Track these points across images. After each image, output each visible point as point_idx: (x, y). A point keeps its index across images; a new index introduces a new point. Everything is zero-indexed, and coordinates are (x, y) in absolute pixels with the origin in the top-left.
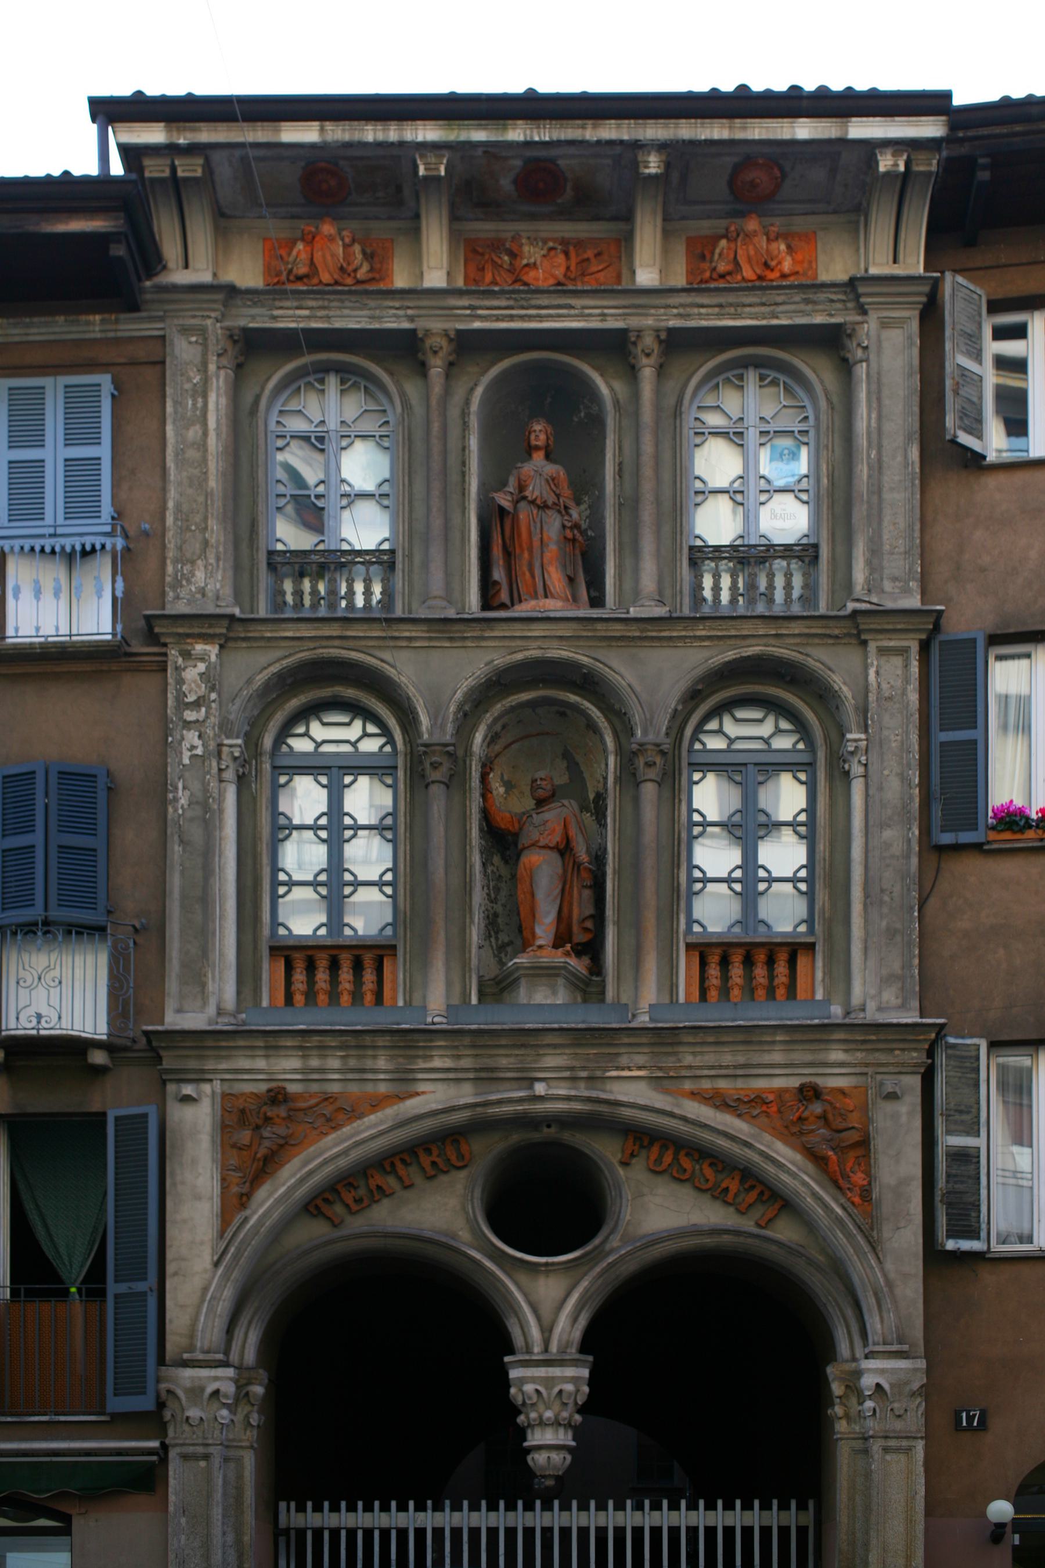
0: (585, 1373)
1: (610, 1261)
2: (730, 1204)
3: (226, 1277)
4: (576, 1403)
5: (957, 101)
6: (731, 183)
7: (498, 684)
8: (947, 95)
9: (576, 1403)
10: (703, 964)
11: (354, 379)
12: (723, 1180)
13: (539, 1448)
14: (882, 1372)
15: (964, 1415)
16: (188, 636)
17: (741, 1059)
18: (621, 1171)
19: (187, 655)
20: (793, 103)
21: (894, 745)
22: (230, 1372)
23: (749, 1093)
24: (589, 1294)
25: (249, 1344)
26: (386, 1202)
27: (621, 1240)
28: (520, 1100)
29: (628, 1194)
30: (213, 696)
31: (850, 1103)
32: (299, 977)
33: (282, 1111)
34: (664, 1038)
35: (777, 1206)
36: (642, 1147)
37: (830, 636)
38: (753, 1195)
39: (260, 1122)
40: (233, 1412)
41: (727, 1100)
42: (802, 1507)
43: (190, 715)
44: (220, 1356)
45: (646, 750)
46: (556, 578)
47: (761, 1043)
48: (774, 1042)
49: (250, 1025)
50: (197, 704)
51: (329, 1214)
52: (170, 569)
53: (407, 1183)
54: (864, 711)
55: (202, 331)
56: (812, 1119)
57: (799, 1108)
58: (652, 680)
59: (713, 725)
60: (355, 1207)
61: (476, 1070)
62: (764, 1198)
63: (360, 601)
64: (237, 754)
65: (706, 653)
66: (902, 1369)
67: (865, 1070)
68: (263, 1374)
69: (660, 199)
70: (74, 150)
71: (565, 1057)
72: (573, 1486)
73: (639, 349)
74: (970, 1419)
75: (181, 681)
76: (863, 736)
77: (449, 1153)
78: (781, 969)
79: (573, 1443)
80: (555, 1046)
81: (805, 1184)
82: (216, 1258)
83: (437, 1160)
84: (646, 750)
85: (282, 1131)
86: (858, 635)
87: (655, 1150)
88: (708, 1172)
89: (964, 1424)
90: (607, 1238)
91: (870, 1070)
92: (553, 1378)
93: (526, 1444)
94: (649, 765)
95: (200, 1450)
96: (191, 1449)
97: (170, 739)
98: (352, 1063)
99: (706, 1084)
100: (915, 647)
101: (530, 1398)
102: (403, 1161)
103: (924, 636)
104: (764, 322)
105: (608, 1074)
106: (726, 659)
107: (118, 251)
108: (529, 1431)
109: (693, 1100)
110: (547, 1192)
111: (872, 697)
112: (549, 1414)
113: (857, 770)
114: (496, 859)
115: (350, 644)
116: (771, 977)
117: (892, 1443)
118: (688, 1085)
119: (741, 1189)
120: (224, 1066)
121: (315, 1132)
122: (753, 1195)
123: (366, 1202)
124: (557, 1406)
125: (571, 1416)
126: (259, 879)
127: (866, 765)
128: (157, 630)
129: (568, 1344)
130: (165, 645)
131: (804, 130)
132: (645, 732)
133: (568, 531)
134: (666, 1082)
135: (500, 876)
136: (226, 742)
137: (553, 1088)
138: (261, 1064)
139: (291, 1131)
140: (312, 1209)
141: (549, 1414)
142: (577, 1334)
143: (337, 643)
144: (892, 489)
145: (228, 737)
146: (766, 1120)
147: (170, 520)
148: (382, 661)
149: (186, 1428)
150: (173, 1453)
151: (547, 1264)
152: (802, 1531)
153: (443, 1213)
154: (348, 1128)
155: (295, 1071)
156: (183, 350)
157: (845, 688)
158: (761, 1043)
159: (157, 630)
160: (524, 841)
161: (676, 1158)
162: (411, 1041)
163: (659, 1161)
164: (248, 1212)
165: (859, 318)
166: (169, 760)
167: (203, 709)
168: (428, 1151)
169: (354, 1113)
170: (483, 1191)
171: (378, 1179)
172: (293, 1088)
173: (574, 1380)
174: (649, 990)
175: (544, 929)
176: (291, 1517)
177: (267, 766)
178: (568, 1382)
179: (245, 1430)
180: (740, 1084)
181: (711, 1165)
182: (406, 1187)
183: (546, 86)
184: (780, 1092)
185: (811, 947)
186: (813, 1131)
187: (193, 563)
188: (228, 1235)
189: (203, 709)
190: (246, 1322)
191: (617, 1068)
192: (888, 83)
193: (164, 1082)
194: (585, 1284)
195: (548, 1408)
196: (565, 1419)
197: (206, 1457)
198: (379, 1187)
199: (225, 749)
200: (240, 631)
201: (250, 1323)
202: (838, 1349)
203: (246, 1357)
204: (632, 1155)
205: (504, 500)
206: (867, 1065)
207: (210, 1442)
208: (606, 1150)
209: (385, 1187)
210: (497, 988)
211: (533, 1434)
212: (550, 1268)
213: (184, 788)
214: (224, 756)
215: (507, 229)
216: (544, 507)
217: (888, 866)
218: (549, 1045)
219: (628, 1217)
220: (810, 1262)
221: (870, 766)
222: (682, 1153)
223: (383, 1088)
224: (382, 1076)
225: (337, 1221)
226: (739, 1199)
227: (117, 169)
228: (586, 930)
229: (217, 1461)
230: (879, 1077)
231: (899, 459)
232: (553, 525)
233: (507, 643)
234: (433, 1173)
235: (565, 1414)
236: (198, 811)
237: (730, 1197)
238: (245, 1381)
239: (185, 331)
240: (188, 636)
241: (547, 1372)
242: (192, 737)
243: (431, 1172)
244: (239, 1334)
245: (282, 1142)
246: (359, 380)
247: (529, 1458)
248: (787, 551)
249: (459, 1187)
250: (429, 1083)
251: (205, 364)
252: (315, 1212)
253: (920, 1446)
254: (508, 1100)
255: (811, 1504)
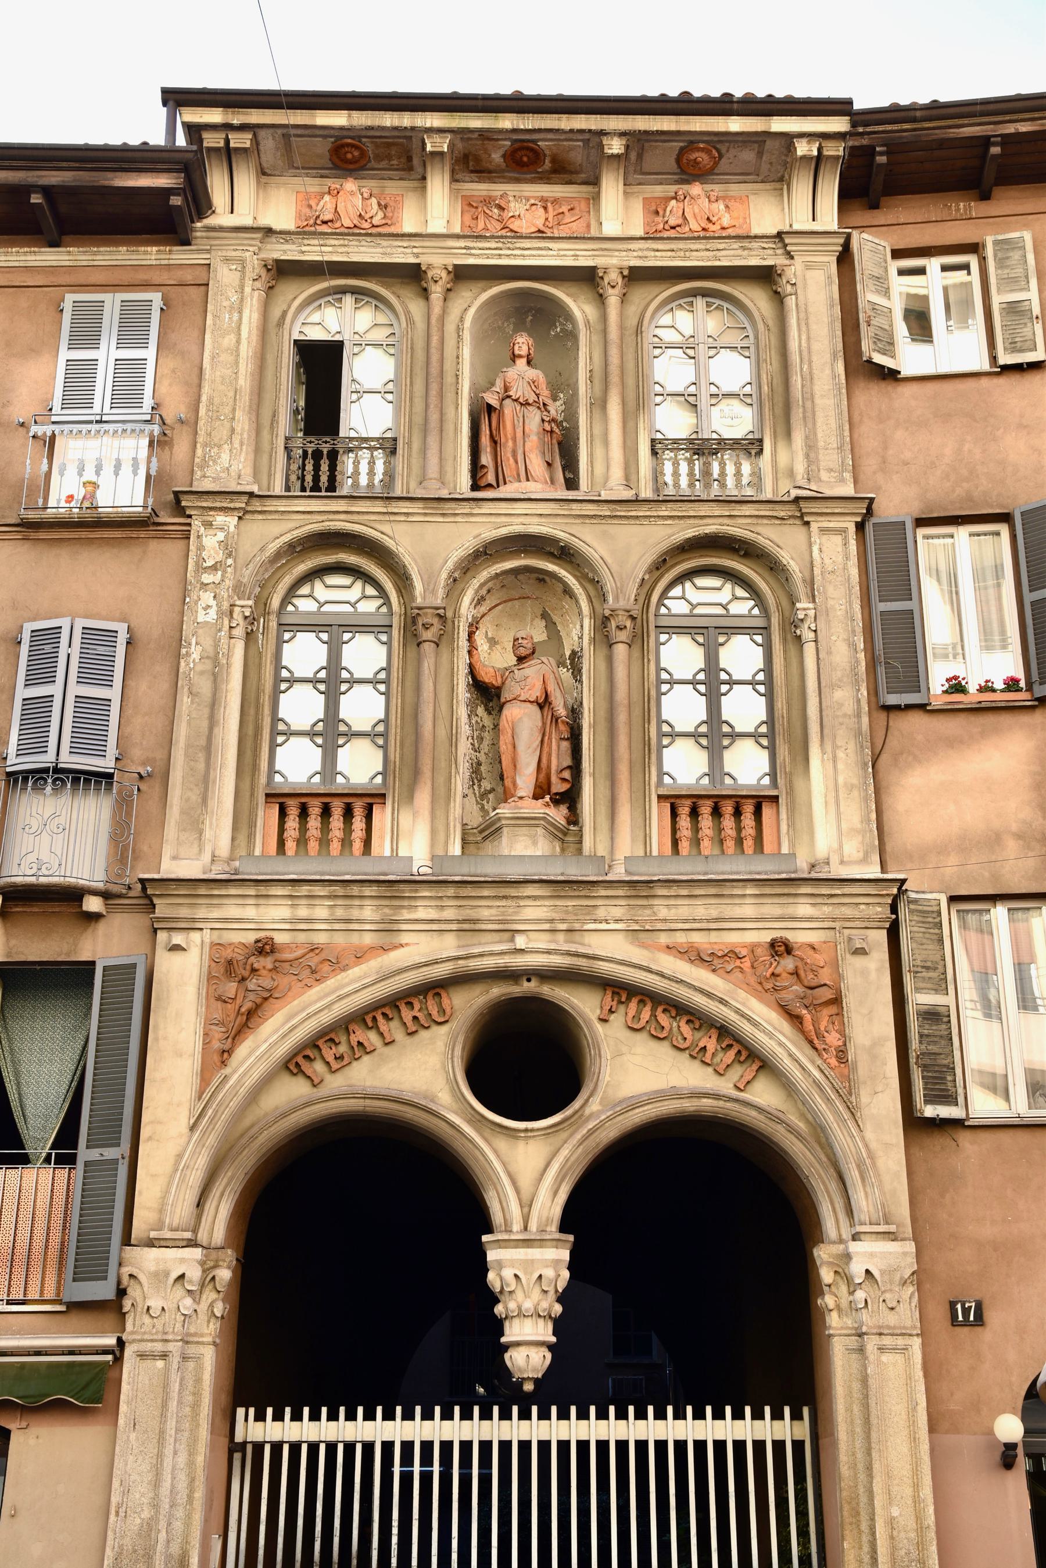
0: (565, 1255)
1: (590, 1127)
2: (708, 1065)
3: (200, 1142)
4: (557, 1291)
5: (857, 106)
6: (678, 161)
7: (485, 553)
8: (849, 102)
9: (557, 1291)
10: (674, 814)
11: (367, 299)
12: (700, 1039)
13: (518, 1344)
14: (872, 1255)
15: (959, 1306)
16: (211, 509)
17: (714, 913)
18: (599, 1027)
19: (208, 525)
20: (725, 106)
21: (839, 613)
22: (197, 1253)
23: (723, 947)
24: (569, 1163)
25: (219, 1219)
26: (366, 1058)
27: (601, 1103)
28: (502, 953)
29: (607, 1052)
30: (230, 561)
31: (820, 959)
32: (292, 823)
33: (267, 962)
34: (639, 888)
35: (755, 1067)
36: (620, 1002)
37: (777, 518)
38: (731, 1054)
39: (246, 974)
40: (197, 1301)
41: (702, 955)
42: (796, 1416)
43: (207, 578)
44: (188, 1235)
45: (617, 615)
46: (537, 465)
47: (732, 896)
48: (744, 895)
49: (244, 874)
50: (214, 568)
51: (309, 1072)
52: (199, 452)
53: (388, 1040)
54: (811, 583)
55: (242, 262)
56: (784, 975)
57: (771, 964)
58: (621, 552)
59: (677, 591)
60: (335, 1065)
61: (459, 921)
62: (742, 1058)
63: (363, 480)
64: (247, 614)
65: (669, 531)
66: (890, 1253)
67: (831, 924)
68: (230, 1256)
69: (622, 171)
70: (148, 126)
71: (545, 909)
72: (554, 1393)
73: (606, 281)
74: (966, 1311)
75: (201, 548)
76: (811, 606)
77: (430, 1008)
78: (748, 820)
79: (554, 1339)
80: (535, 898)
81: (781, 1044)
82: (192, 1121)
83: (418, 1015)
84: (617, 615)
85: (267, 983)
86: (802, 517)
87: (633, 1005)
88: (686, 1029)
89: (960, 1318)
90: (587, 1101)
91: (837, 925)
92: (532, 1261)
93: (503, 1340)
94: (620, 628)
95: (159, 1347)
96: (148, 1347)
97: (188, 600)
98: (340, 913)
99: (681, 938)
100: (852, 528)
101: (508, 1285)
102: (384, 1015)
103: (859, 519)
104: (709, 264)
105: (586, 927)
106: (687, 536)
107: (176, 201)
108: (507, 1324)
109: (670, 954)
110: (526, 1057)
111: (817, 571)
112: (528, 1305)
113: (808, 635)
114: (481, 710)
115: (355, 517)
116: (739, 829)
117: (887, 1341)
118: (664, 939)
119: (719, 1048)
120: (216, 914)
121: (300, 984)
122: (731, 1054)
123: (346, 1061)
124: (536, 1294)
125: (551, 1307)
126: (261, 730)
127: (815, 631)
128: (183, 504)
129: (549, 1222)
130: (190, 516)
131: (735, 124)
132: (616, 598)
133: (546, 424)
134: (642, 935)
135: (483, 726)
136: (238, 603)
137: (534, 938)
138: (250, 912)
139: (276, 983)
140: (292, 1067)
141: (528, 1305)
142: (557, 1211)
143: (343, 517)
144: (822, 396)
145: (239, 599)
146: (740, 975)
147: (202, 411)
148: (382, 533)
149: (147, 1320)
150: (129, 1352)
151: (526, 1130)
152: (798, 1445)
153: (422, 1074)
154: (333, 980)
155: (284, 921)
156: (225, 276)
157: (792, 563)
158: (732, 896)
159: (183, 504)
160: (506, 695)
161: (654, 1015)
162: (396, 888)
163: (637, 1017)
164: (227, 1071)
165: (787, 262)
166: (185, 618)
167: (220, 573)
168: (410, 1005)
169: (338, 965)
170: (463, 1048)
171: (359, 1034)
172: (280, 938)
173: (556, 1262)
174: (624, 837)
175: (525, 781)
176: (254, 1429)
177: (273, 624)
178: (547, 1266)
179: (209, 1322)
180: (714, 937)
181: (688, 1022)
182: (387, 1044)
183: (529, 91)
184: (753, 948)
185: (775, 799)
186: (785, 988)
187: (220, 446)
188: (206, 1096)
189: (220, 573)
190: (218, 1194)
191: (595, 921)
192: (800, 93)
193: (155, 931)
194: (565, 1152)
195: (527, 1296)
196: (545, 1310)
197: (164, 1356)
198: (360, 1044)
199: (237, 610)
200: (256, 505)
201: (222, 1195)
202: (824, 1228)
203: (215, 1235)
204: (611, 1011)
205: (492, 400)
206: (834, 920)
207: (170, 1337)
208: (583, 1005)
209: (366, 1044)
210: (483, 834)
211: (511, 1327)
212: (530, 1134)
213: (197, 644)
214: (235, 616)
215: (497, 189)
216: (527, 404)
217: (841, 724)
218: (529, 897)
219: (607, 1078)
220: (791, 1129)
221: (819, 632)
222: (660, 1009)
223: (368, 939)
224: (368, 927)
225: (316, 1081)
226: (717, 1059)
227: (181, 141)
228: (564, 780)
229: (175, 1360)
230: (847, 932)
231: (828, 371)
232: (534, 419)
233: (493, 519)
234: (414, 1029)
235: (545, 1305)
236: (208, 665)
237: (708, 1058)
238: (212, 1264)
239: (227, 260)
240: (211, 509)
241: (526, 1254)
242: (207, 598)
243: (412, 1027)
244: (210, 1206)
245: (266, 995)
246: (370, 300)
247: (507, 1356)
248: (735, 445)
249: (440, 1045)
250: (412, 934)
251: (242, 287)
252: (295, 1071)
253: (917, 1342)
254: (490, 953)
255: (806, 1411)
